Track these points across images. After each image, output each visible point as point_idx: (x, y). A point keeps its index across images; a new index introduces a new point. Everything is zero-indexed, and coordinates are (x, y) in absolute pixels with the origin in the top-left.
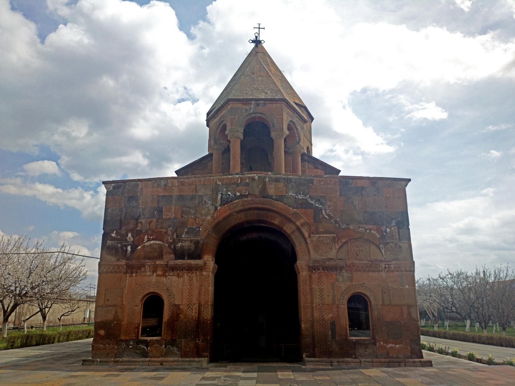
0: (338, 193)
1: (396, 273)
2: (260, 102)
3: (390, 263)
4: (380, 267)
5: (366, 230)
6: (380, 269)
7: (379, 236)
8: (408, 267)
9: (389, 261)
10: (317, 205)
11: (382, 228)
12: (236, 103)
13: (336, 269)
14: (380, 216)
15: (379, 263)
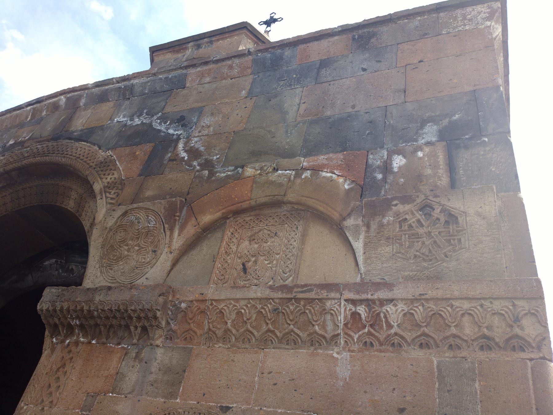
0: (244, 92)
1: (417, 354)
2: (201, 41)
3: (382, 294)
4: (328, 317)
5: (299, 171)
6: (324, 326)
7: (346, 187)
8: (496, 321)
9: (377, 286)
10: (171, 131)
11: (371, 156)
12: (163, 54)
13: (127, 327)
14: (371, 122)
15: (324, 294)
